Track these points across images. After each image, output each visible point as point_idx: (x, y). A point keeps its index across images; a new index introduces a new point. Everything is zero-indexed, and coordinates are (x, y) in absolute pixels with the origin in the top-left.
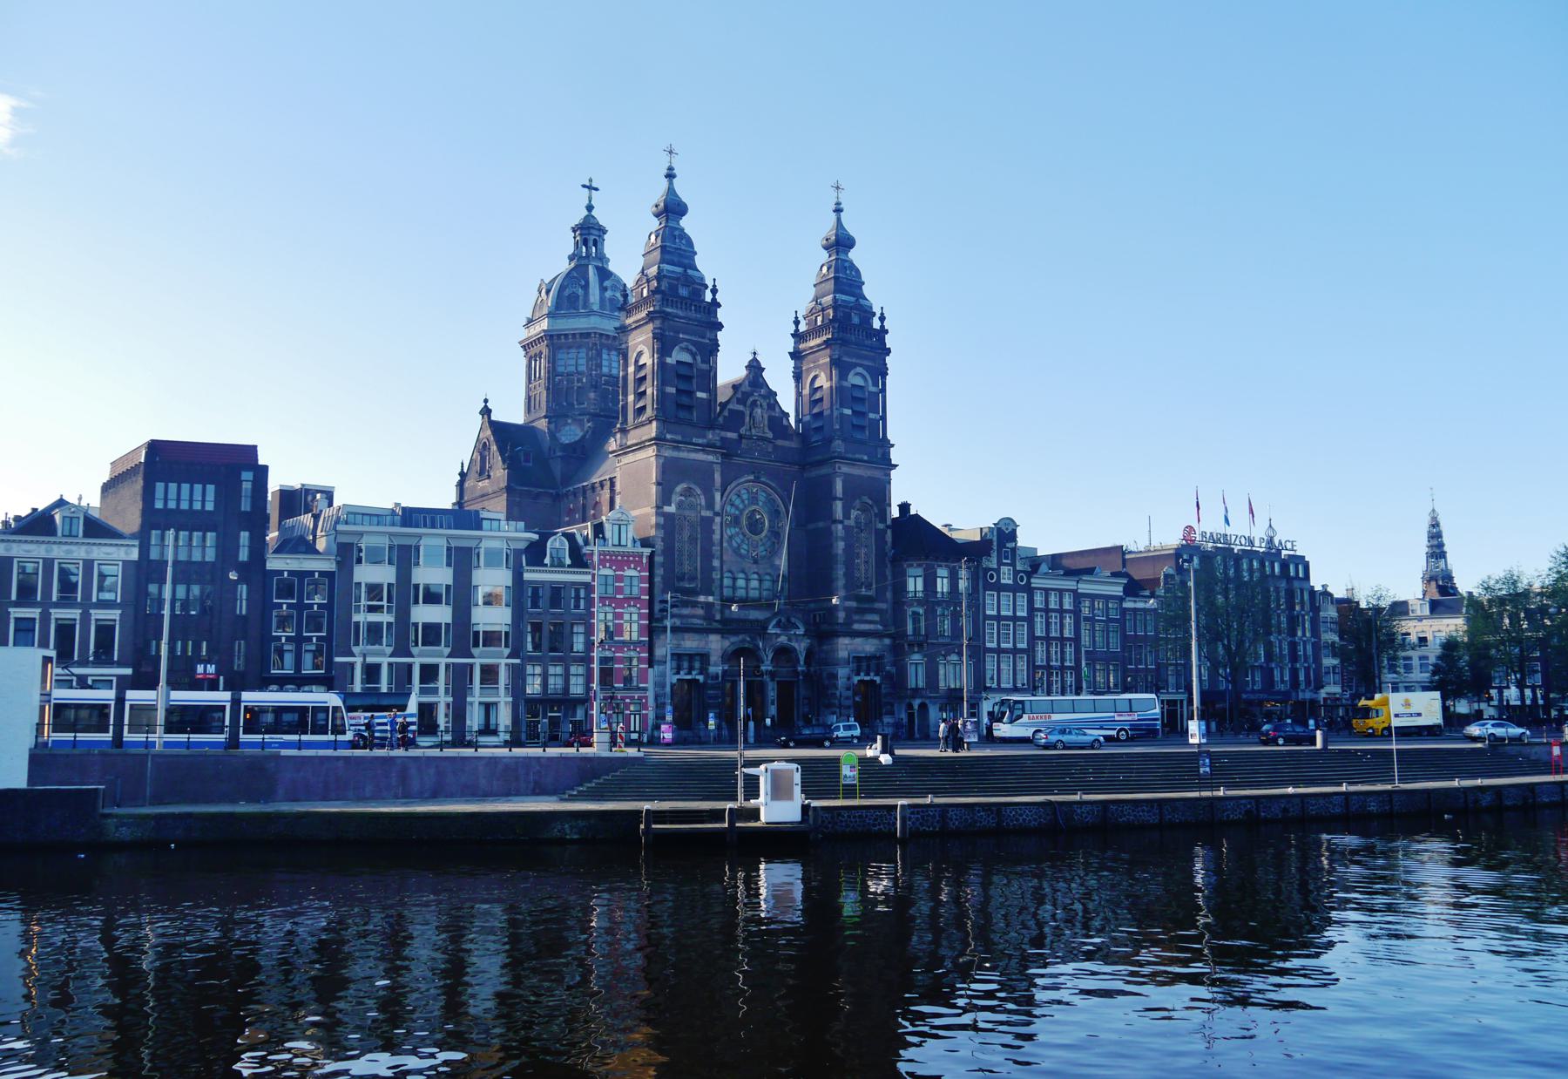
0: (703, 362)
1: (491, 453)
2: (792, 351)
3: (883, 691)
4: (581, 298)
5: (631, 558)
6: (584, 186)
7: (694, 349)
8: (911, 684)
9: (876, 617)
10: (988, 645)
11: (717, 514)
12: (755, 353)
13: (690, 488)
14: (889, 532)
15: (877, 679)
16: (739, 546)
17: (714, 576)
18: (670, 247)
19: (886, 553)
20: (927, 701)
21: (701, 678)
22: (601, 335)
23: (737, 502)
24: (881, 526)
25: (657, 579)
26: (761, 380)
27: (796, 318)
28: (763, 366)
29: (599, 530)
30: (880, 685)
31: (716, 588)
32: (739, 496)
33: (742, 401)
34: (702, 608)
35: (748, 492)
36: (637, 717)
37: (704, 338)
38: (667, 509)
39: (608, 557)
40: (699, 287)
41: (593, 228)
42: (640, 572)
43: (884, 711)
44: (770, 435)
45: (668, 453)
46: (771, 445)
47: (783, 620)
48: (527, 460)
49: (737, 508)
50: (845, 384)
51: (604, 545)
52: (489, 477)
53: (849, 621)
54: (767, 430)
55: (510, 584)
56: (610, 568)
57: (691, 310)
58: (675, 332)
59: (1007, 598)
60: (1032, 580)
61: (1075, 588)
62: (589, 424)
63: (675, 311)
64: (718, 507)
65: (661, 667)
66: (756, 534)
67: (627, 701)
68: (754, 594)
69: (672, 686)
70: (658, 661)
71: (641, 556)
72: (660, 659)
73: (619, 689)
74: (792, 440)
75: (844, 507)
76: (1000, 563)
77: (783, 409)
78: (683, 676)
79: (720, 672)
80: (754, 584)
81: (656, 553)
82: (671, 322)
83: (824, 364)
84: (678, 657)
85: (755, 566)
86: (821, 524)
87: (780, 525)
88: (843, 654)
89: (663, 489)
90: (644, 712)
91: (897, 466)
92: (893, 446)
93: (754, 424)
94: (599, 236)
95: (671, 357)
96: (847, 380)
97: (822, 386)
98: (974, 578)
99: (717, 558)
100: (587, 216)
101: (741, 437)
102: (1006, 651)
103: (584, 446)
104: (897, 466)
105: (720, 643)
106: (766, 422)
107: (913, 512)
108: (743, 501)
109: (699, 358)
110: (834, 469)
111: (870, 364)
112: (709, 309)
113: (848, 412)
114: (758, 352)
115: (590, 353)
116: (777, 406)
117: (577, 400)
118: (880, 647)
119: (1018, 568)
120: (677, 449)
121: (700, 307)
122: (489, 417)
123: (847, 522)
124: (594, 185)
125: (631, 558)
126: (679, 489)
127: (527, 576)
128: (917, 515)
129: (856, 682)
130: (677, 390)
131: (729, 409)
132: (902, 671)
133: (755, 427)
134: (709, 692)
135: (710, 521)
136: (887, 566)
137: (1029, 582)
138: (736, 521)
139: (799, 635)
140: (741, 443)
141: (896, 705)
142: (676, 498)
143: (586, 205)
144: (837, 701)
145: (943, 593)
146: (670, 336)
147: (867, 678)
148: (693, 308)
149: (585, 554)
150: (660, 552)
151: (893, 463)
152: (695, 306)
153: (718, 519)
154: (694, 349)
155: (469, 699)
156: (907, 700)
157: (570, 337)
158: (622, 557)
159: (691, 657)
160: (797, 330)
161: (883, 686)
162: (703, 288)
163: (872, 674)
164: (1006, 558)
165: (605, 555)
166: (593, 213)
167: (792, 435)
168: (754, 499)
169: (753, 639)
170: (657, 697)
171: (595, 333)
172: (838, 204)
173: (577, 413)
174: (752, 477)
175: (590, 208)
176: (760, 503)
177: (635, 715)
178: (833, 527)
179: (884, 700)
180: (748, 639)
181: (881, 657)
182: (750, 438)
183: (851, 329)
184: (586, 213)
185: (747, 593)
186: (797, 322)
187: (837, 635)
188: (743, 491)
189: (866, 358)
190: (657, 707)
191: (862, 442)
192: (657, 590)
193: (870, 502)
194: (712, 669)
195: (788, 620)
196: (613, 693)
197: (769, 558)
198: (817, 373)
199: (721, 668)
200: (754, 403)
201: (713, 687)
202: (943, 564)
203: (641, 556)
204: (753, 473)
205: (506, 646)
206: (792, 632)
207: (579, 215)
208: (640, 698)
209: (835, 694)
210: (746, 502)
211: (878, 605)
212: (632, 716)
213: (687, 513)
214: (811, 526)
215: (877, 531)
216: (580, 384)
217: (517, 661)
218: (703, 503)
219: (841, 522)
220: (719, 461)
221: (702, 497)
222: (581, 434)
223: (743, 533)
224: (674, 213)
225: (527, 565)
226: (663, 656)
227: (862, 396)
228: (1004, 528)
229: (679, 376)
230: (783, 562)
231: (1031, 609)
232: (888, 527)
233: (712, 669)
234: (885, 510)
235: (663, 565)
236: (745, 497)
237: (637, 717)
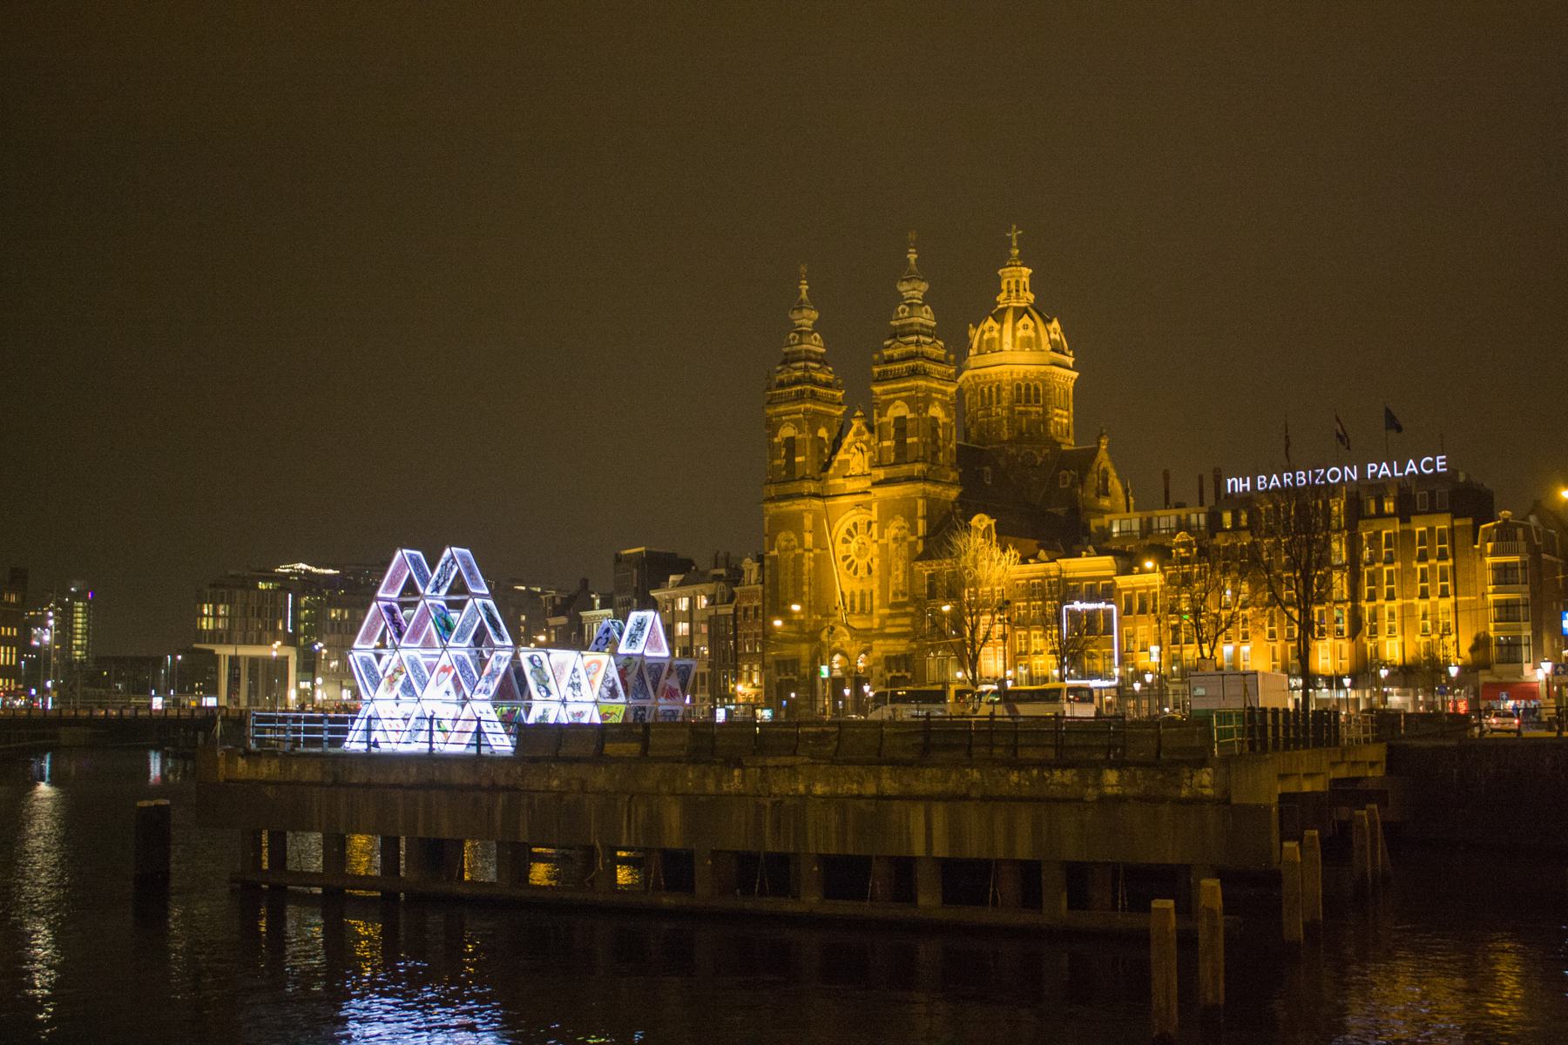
0: (799, 433)
14: (921, 542)
21: (795, 678)
24: (913, 538)
25: (767, 606)
34: (796, 624)
38: (772, 553)
50: (884, 419)
65: (768, 671)
71: (757, 591)
75: (878, 528)
78: (784, 677)
95: (777, 436)
96: (886, 416)
123: (881, 541)
129: (889, 679)
135: (803, 555)
194: (802, 670)
215: (910, 544)
232: (919, 538)
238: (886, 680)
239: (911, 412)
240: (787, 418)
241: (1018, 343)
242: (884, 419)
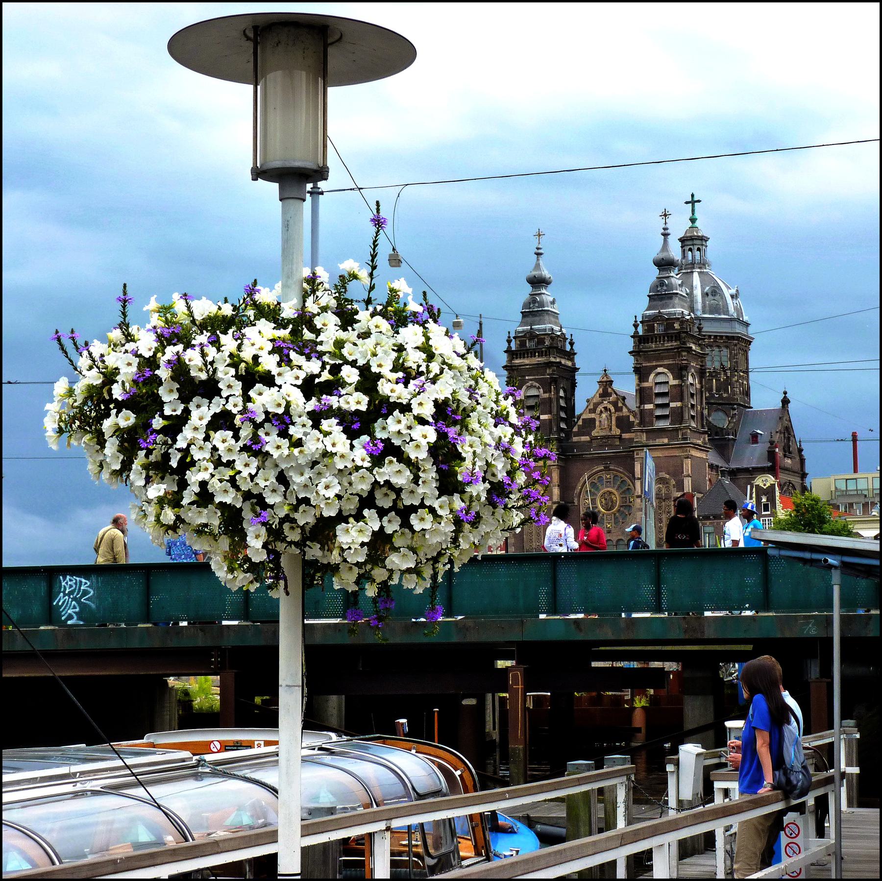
0: (544, 392)
6: (687, 203)
11: (554, 503)
26: (610, 390)
33: (593, 411)
41: (687, 240)
42: (501, 550)
44: (618, 432)
50: (645, 385)
54: (614, 427)
63: (522, 361)
94: (693, 245)
96: (647, 381)
106: (614, 422)
109: (541, 390)
111: (671, 362)
113: (650, 406)
119: (772, 518)
121: (542, 352)
124: (696, 199)
131: (583, 419)
133: (602, 429)
148: (537, 354)
152: (538, 352)
154: (537, 385)
162: (546, 337)
164: (766, 509)
166: (697, 224)
175: (693, 220)
182: (596, 438)
183: (652, 339)
184: (690, 224)
191: (662, 431)
193: (668, 476)
202: (708, 522)
220: (556, 464)
234: (683, 479)
239: (674, 379)
240: (531, 377)
241: (707, 308)
242: (645, 385)
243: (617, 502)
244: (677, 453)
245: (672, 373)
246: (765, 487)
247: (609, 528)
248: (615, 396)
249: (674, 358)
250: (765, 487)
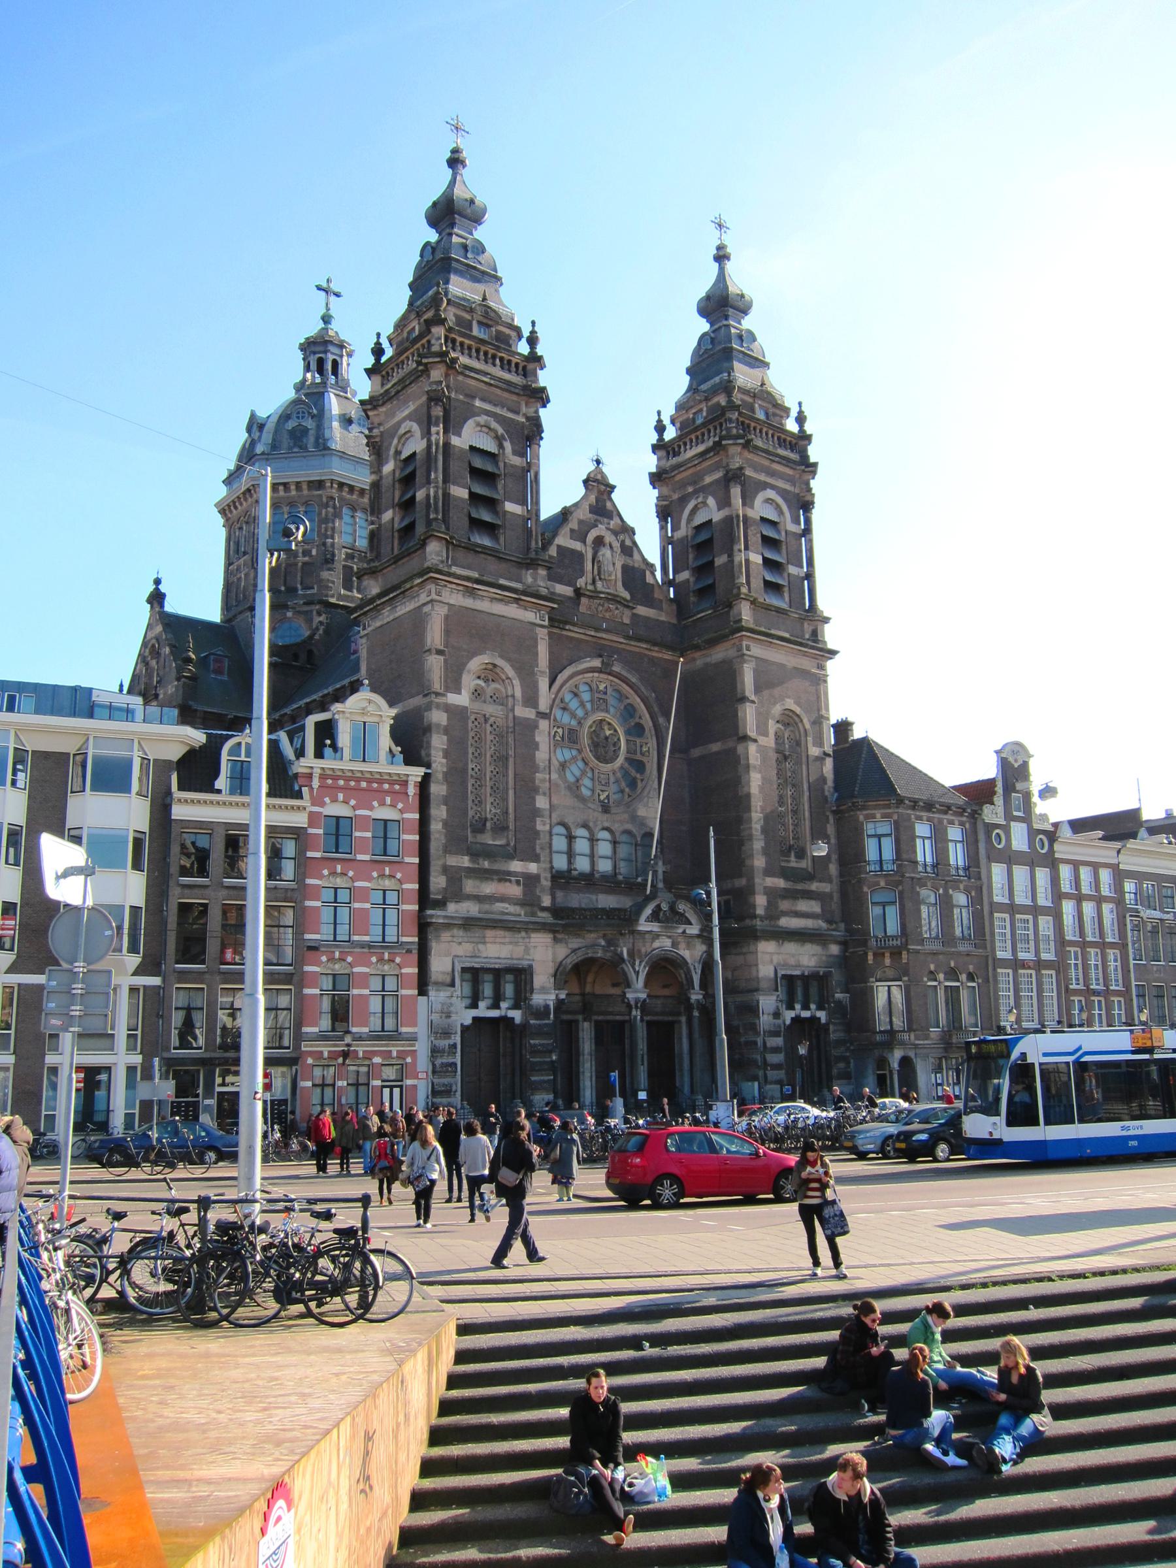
0: (515, 453)
1: (162, 659)
2: (654, 470)
3: (833, 1037)
4: (312, 432)
5: (386, 786)
6: (319, 288)
7: (500, 431)
8: (882, 1024)
9: (815, 907)
10: (1000, 954)
12: (598, 462)
13: (495, 666)
14: (829, 764)
15: (822, 1015)
16: (578, 781)
17: (539, 827)
18: (457, 261)
19: (826, 797)
20: (911, 1054)
21: (517, 1015)
22: (341, 485)
23: (574, 704)
25: (436, 827)
26: (608, 504)
27: (660, 421)
28: (612, 482)
29: (326, 731)
30: (827, 1024)
31: (542, 848)
32: (576, 695)
33: (581, 536)
34: (518, 882)
35: (591, 690)
36: (396, 1091)
37: (517, 412)
38: (453, 699)
39: (341, 782)
40: (507, 331)
43: (835, 1071)
45: (457, 599)
46: (627, 612)
47: (665, 907)
48: (219, 671)
49: (573, 715)
51: (335, 759)
52: (156, 696)
53: (773, 913)
54: (620, 584)
55: (145, 828)
56: (346, 802)
57: (494, 365)
58: (466, 395)
59: (1020, 873)
60: (1056, 847)
61: (1115, 861)
62: (321, 619)
64: (544, 705)
66: (606, 761)
67: (377, 1060)
68: (605, 866)
69: (465, 1029)
70: (436, 983)
72: (440, 978)
73: (359, 1038)
74: (661, 609)
75: (758, 714)
76: (1009, 817)
77: (646, 557)
79: (551, 1004)
80: (604, 848)
81: (433, 779)
82: (460, 378)
83: (711, 484)
84: (474, 975)
85: (606, 816)
86: (715, 747)
87: (644, 749)
88: (765, 971)
89: (445, 661)
90: (409, 1082)
91: (833, 653)
92: (826, 620)
93: (599, 574)
95: (460, 436)
96: (752, 507)
97: (711, 521)
98: (971, 842)
99: (544, 794)
100: (323, 329)
101: (578, 593)
102: (1023, 965)
103: (310, 652)
104: (833, 653)
105: (550, 952)
107: (857, 733)
108: (582, 704)
109: (508, 445)
110: (740, 649)
111: (787, 486)
112: (524, 368)
114: (603, 459)
115: (324, 511)
116: (635, 549)
117: (301, 584)
118: (824, 958)
119: (1036, 826)
120: (471, 592)
121: (509, 362)
122: (162, 605)
124: (334, 287)
125: (386, 786)
126: (476, 664)
127: (179, 812)
128: (865, 743)
129: (788, 1022)
130: (472, 495)
131: (559, 547)
132: (864, 1000)
134: (532, 1042)
135: (532, 726)
136: (828, 821)
137: (1051, 849)
138: (572, 737)
139: (692, 937)
140: (579, 604)
141: (852, 1061)
142: (469, 681)
143: (322, 314)
144: (759, 1057)
145: (925, 865)
146: (458, 400)
147: (806, 1014)
149: (296, 776)
150: (440, 776)
151: (830, 646)
152: (502, 359)
153: (544, 724)
154: (500, 431)
155: (50, 1059)
156: (877, 1053)
157: (293, 487)
158: (369, 781)
159: (498, 974)
160: (661, 439)
161: (831, 1027)
162: (513, 334)
163: (813, 1006)
165: (336, 778)
167: (661, 601)
168: (600, 702)
169: (611, 943)
170: (435, 1052)
171: (332, 481)
172: (720, 248)
173: (302, 602)
174: (597, 663)
175: (326, 319)
176: (612, 710)
177: (391, 1088)
178: (740, 749)
179: (835, 1052)
180: (603, 943)
181: (827, 975)
182: (594, 595)
184: (321, 325)
185: (593, 863)
186: (660, 428)
187: (755, 935)
188: (583, 688)
189: (782, 476)
190: (434, 1072)
192: (435, 846)
194: (538, 999)
195: (672, 908)
196: (348, 1045)
197: (628, 805)
198: (700, 500)
199: (553, 997)
200: (599, 542)
201: (539, 1032)
202: (924, 814)
203: (405, 783)
204: (600, 656)
205: (133, 949)
206: (680, 931)
207: (313, 328)
208: (402, 1055)
209: (755, 1043)
210: (588, 706)
211: (814, 886)
212: (386, 1091)
213: (491, 709)
214: (696, 752)
216: (306, 559)
217: (155, 981)
218: (518, 693)
219: (755, 741)
221: (516, 682)
222: (307, 633)
223: (583, 760)
224: (465, 217)
225: (181, 788)
226: (444, 973)
227: (776, 537)
228: (1011, 759)
229: (475, 473)
230: (652, 811)
231: (1058, 896)
233: (538, 999)
235: (446, 801)
236: (586, 697)
237: (396, 1091)
238: (785, 1024)
243: (616, 744)
244: (807, 664)
245: (789, 507)
246: (1016, 765)
247: (603, 802)
248: (619, 521)
249: (791, 480)
250: (1016, 765)
